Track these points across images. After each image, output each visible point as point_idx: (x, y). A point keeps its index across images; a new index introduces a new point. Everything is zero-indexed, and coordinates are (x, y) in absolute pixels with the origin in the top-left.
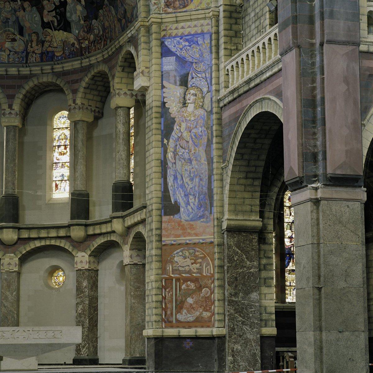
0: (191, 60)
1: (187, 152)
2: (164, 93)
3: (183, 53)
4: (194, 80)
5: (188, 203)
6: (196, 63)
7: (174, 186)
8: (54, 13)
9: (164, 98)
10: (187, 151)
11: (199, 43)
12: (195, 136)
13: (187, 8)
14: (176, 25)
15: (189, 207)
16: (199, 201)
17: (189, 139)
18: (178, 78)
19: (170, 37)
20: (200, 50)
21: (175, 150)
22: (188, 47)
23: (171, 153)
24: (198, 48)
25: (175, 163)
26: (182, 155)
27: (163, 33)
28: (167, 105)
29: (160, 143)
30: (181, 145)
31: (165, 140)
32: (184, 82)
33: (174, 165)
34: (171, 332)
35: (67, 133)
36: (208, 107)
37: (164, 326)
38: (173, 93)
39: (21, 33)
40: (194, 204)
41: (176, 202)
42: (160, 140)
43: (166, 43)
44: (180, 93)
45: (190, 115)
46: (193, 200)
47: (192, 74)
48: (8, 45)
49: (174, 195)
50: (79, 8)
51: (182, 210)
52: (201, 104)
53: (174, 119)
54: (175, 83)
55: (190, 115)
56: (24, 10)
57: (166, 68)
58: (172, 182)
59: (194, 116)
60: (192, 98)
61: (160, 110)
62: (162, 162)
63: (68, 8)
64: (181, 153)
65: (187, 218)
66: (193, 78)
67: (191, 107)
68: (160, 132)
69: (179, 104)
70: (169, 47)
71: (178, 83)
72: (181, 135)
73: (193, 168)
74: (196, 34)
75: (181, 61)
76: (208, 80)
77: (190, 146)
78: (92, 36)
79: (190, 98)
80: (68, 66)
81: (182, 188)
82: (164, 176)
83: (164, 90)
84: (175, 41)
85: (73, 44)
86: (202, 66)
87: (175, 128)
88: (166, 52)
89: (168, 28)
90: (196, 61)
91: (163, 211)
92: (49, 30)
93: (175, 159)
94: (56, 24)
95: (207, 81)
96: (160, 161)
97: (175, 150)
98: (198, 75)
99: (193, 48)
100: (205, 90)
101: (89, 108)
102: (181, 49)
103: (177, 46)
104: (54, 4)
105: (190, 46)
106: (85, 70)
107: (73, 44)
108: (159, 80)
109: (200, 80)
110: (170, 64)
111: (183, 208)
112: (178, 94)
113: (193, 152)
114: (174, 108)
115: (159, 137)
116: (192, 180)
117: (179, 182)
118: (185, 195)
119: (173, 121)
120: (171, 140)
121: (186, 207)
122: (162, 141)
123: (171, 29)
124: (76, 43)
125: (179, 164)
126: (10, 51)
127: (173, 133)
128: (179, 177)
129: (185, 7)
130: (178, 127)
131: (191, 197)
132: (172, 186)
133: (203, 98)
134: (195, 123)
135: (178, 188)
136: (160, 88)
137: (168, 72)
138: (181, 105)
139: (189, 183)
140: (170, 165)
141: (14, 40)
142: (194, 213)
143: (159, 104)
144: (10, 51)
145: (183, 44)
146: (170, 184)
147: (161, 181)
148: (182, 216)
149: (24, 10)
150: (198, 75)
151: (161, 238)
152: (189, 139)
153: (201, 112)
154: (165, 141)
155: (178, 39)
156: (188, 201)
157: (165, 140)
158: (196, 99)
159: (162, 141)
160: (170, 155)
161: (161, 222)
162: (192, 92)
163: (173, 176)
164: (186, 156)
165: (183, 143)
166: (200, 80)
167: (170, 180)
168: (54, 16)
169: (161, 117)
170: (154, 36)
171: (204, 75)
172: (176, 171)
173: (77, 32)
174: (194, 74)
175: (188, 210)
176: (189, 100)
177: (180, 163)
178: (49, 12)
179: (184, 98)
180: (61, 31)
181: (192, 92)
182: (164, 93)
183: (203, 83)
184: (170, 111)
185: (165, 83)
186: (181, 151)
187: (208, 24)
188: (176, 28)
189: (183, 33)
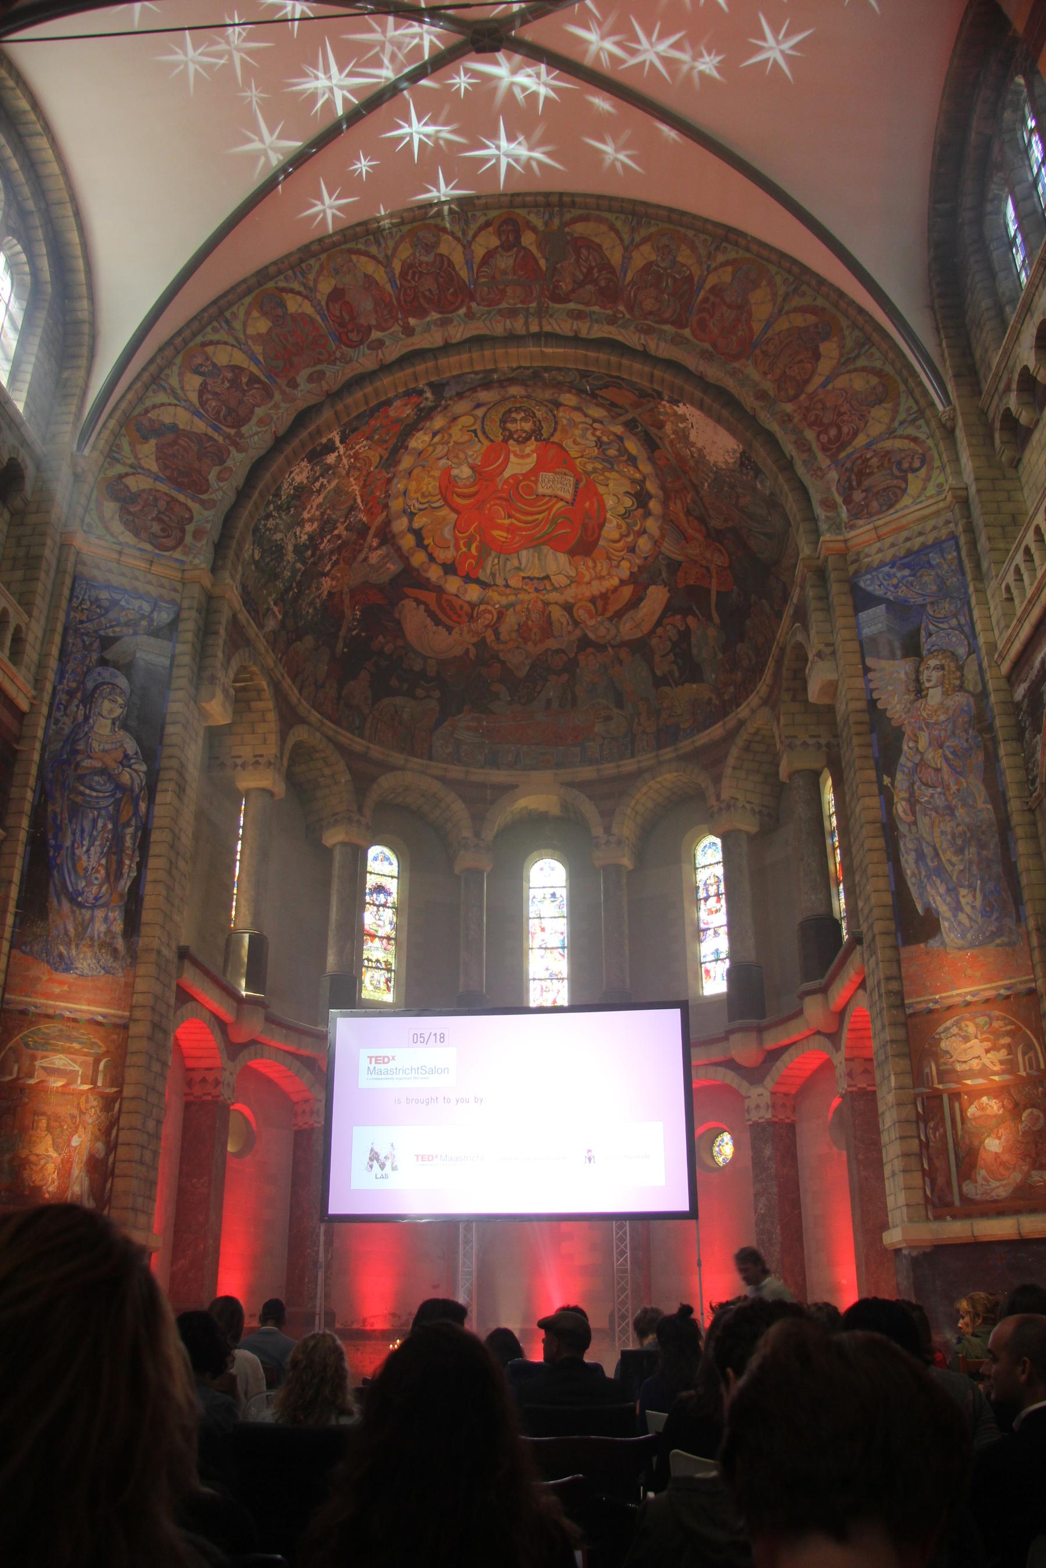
0: (920, 600)
1: (940, 793)
2: (870, 681)
3: (902, 592)
4: (934, 638)
5: (957, 908)
6: (932, 603)
7: (920, 873)
8: (671, 657)
9: (872, 691)
10: (939, 790)
11: (934, 563)
12: (954, 753)
13: (898, 507)
14: (878, 545)
15: (962, 917)
16: (985, 897)
17: (939, 762)
18: (897, 644)
19: (870, 569)
20: (937, 575)
21: (912, 794)
22: (911, 579)
23: (904, 803)
24: (933, 573)
25: (915, 823)
26: (928, 802)
27: (852, 569)
28: (880, 705)
29: (875, 788)
30: (924, 780)
31: (885, 777)
32: (912, 649)
33: (914, 828)
34: (955, 1230)
35: (719, 871)
36: (976, 685)
37: (930, 1216)
38: (892, 675)
39: (620, 704)
40: (973, 907)
41: (928, 910)
42: (874, 779)
43: (862, 584)
44: (906, 673)
45: (936, 711)
46: (969, 899)
47: (927, 628)
48: (598, 728)
49: (921, 895)
50: (712, 632)
51: (945, 925)
52: (957, 682)
53: (899, 728)
54: (893, 656)
55: (936, 711)
56: (621, 662)
57: (866, 631)
58: (914, 866)
59: (946, 713)
60: (935, 675)
61: (866, 718)
62: (884, 827)
63: (693, 640)
64: (926, 798)
65: (960, 942)
66: (930, 635)
67: (935, 696)
68: (872, 763)
69: (906, 697)
70: (870, 589)
71: (899, 653)
72: (922, 759)
73: (958, 825)
74: (924, 548)
75: (899, 609)
76: (966, 629)
77: (946, 777)
78: (739, 674)
79: (931, 676)
80: (703, 738)
81: (939, 876)
82: (893, 855)
83: (870, 676)
84: (880, 576)
85: (710, 699)
86: (947, 606)
87: (905, 748)
88: (862, 600)
89: (862, 556)
90: (933, 599)
91: (899, 935)
92: (667, 689)
93: (914, 813)
94: (677, 674)
95: (962, 632)
96: (878, 825)
97: (912, 794)
98: (941, 625)
99: (921, 576)
100: (962, 651)
101: (748, 806)
102: (896, 586)
103: (885, 583)
104: (670, 640)
105: (914, 575)
106: (730, 737)
107: (710, 699)
108: (856, 658)
109: (948, 635)
110: (874, 621)
111: (947, 919)
112: (903, 676)
113: (954, 788)
114: (895, 705)
115: (872, 774)
116: (960, 851)
117: (931, 864)
118: (949, 891)
119: (898, 734)
120: (899, 776)
121: (955, 916)
122: (880, 781)
123: (868, 556)
124: (714, 697)
125: (924, 822)
126: (604, 738)
127: (902, 760)
128: (928, 851)
129: (891, 506)
130: (911, 744)
131: (963, 892)
132: (914, 875)
133: (960, 668)
134: (950, 725)
135: (929, 877)
136: (861, 672)
137: (873, 639)
138: (912, 697)
139: (954, 859)
140: (903, 828)
141: (608, 718)
142: (976, 926)
143: (861, 705)
144: (604, 738)
145: (899, 575)
146: (909, 872)
147: (886, 868)
148: (947, 940)
149: (621, 662)
150: (941, 625)
151: (903, 1000)
152: (939, 762)
153: (960, 698)
154: (887, 780)
155: (886, 569)
156: (958, 902)
157: (885, 777)
158: (944, 675)
159: (880, 781)
160: (901, 808)
161: (898, 962)
162: (933, 663)
163: (913, 854)
164: (940, 802)
165: (930, 776)
166: (948, 635)
167: (908, 862)
168: (673, 662)
169: (872, 731)
170: (833, 576)
171: (954, 622)
172: (919, 840)
173: (713, 676)
174: (931, 627)
175: (960, 923)
176: (929, 681)
177: (927, 820)
178: (662, 656)
179: (917, 680)
180: (687, 685)
181: (933, 663)
182: (870, 681)
183: (954, 639)
184: (889, 714)
185: (870, 662)
186: (925, 794)
187: (947, 522)
188: (880, 551)
189: (894, 556)
